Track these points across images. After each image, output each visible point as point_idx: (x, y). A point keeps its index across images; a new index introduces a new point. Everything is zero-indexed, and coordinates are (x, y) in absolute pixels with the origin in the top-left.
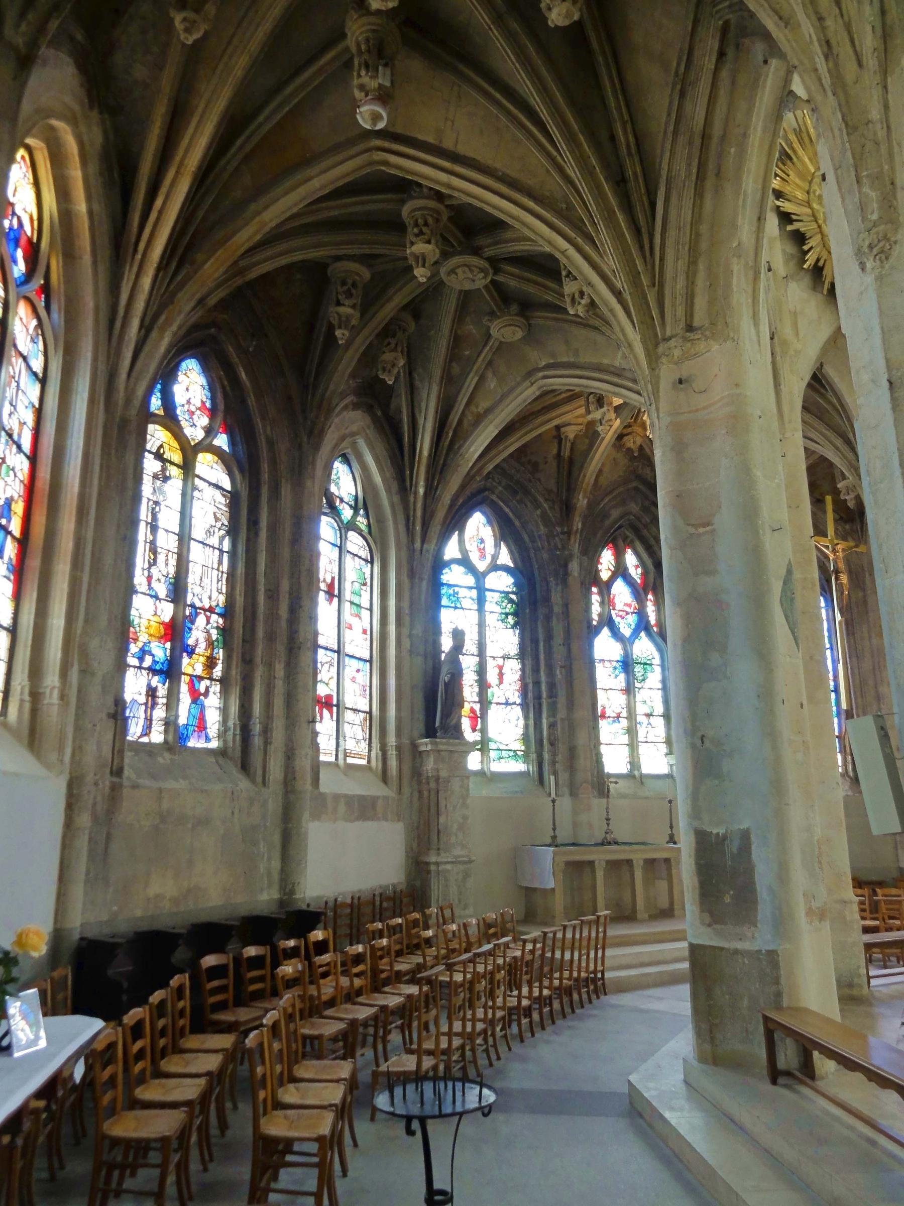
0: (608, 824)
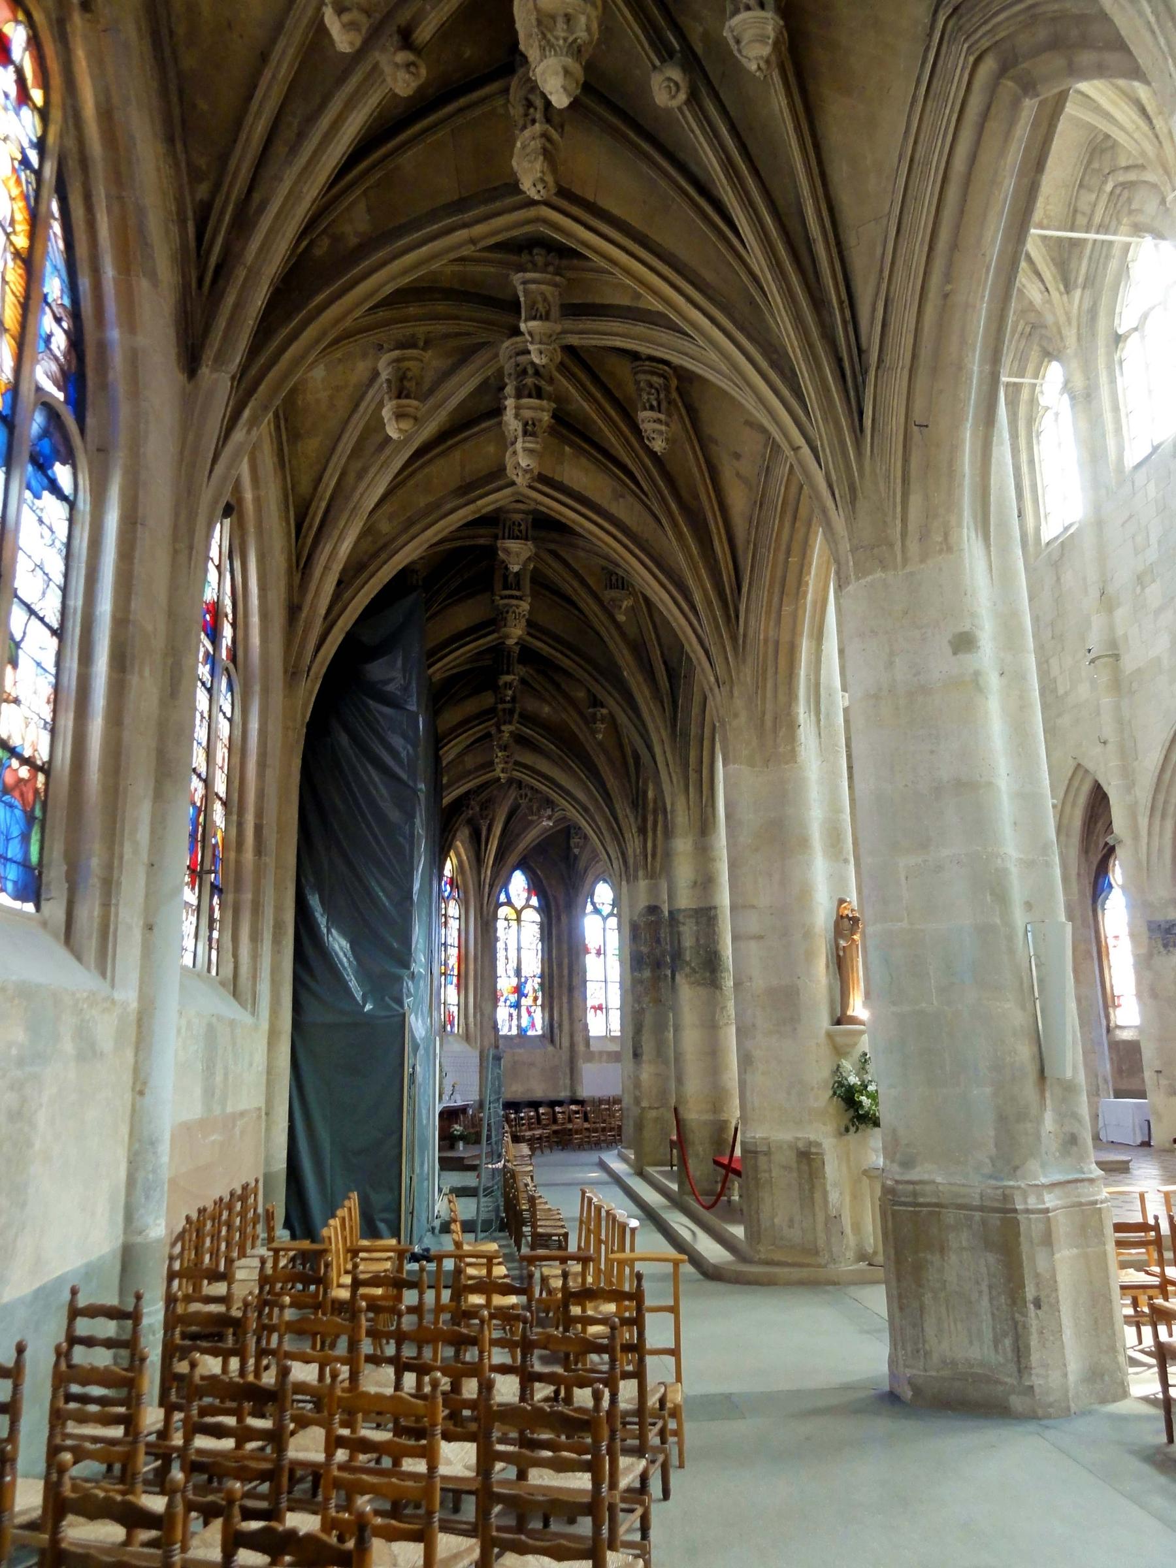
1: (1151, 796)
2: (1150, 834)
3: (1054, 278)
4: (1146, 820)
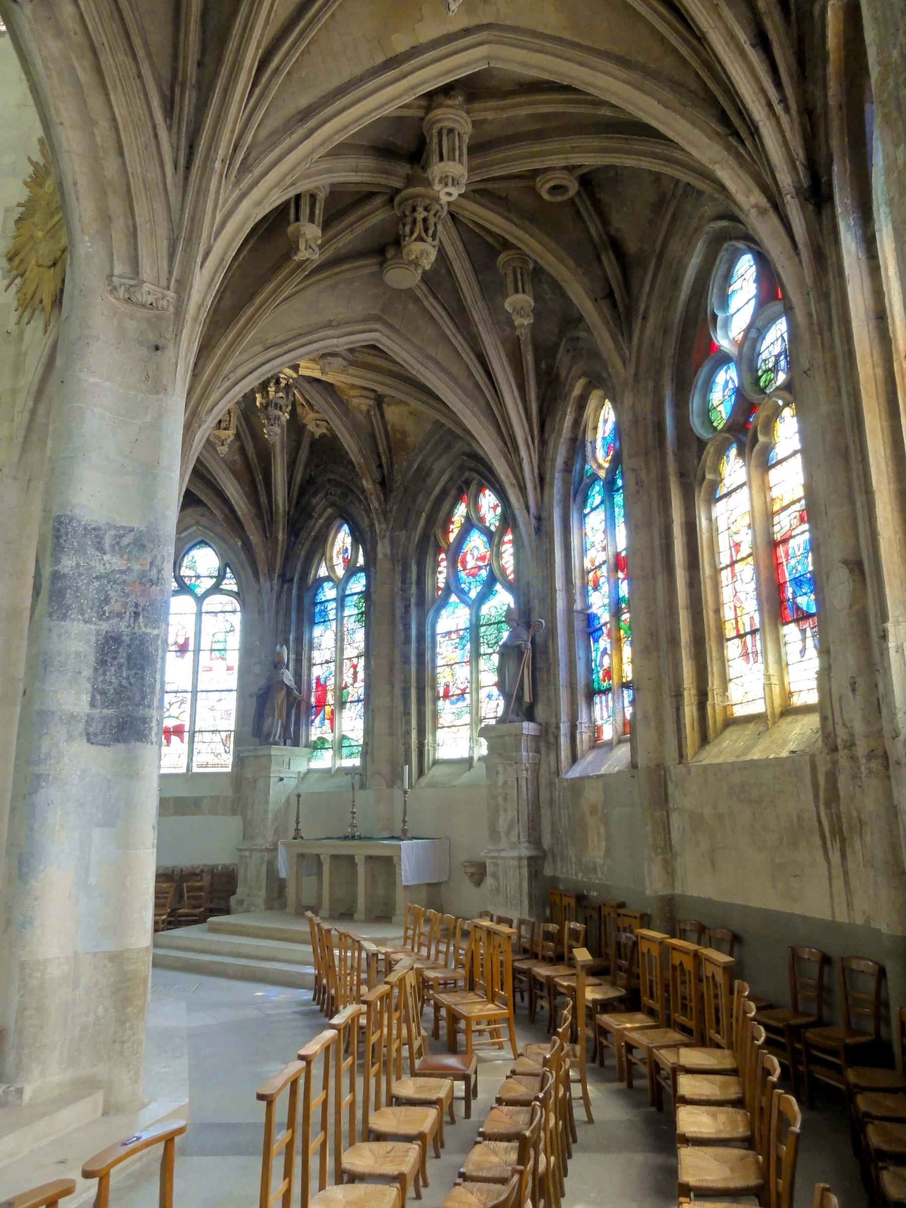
0: (353, 818)
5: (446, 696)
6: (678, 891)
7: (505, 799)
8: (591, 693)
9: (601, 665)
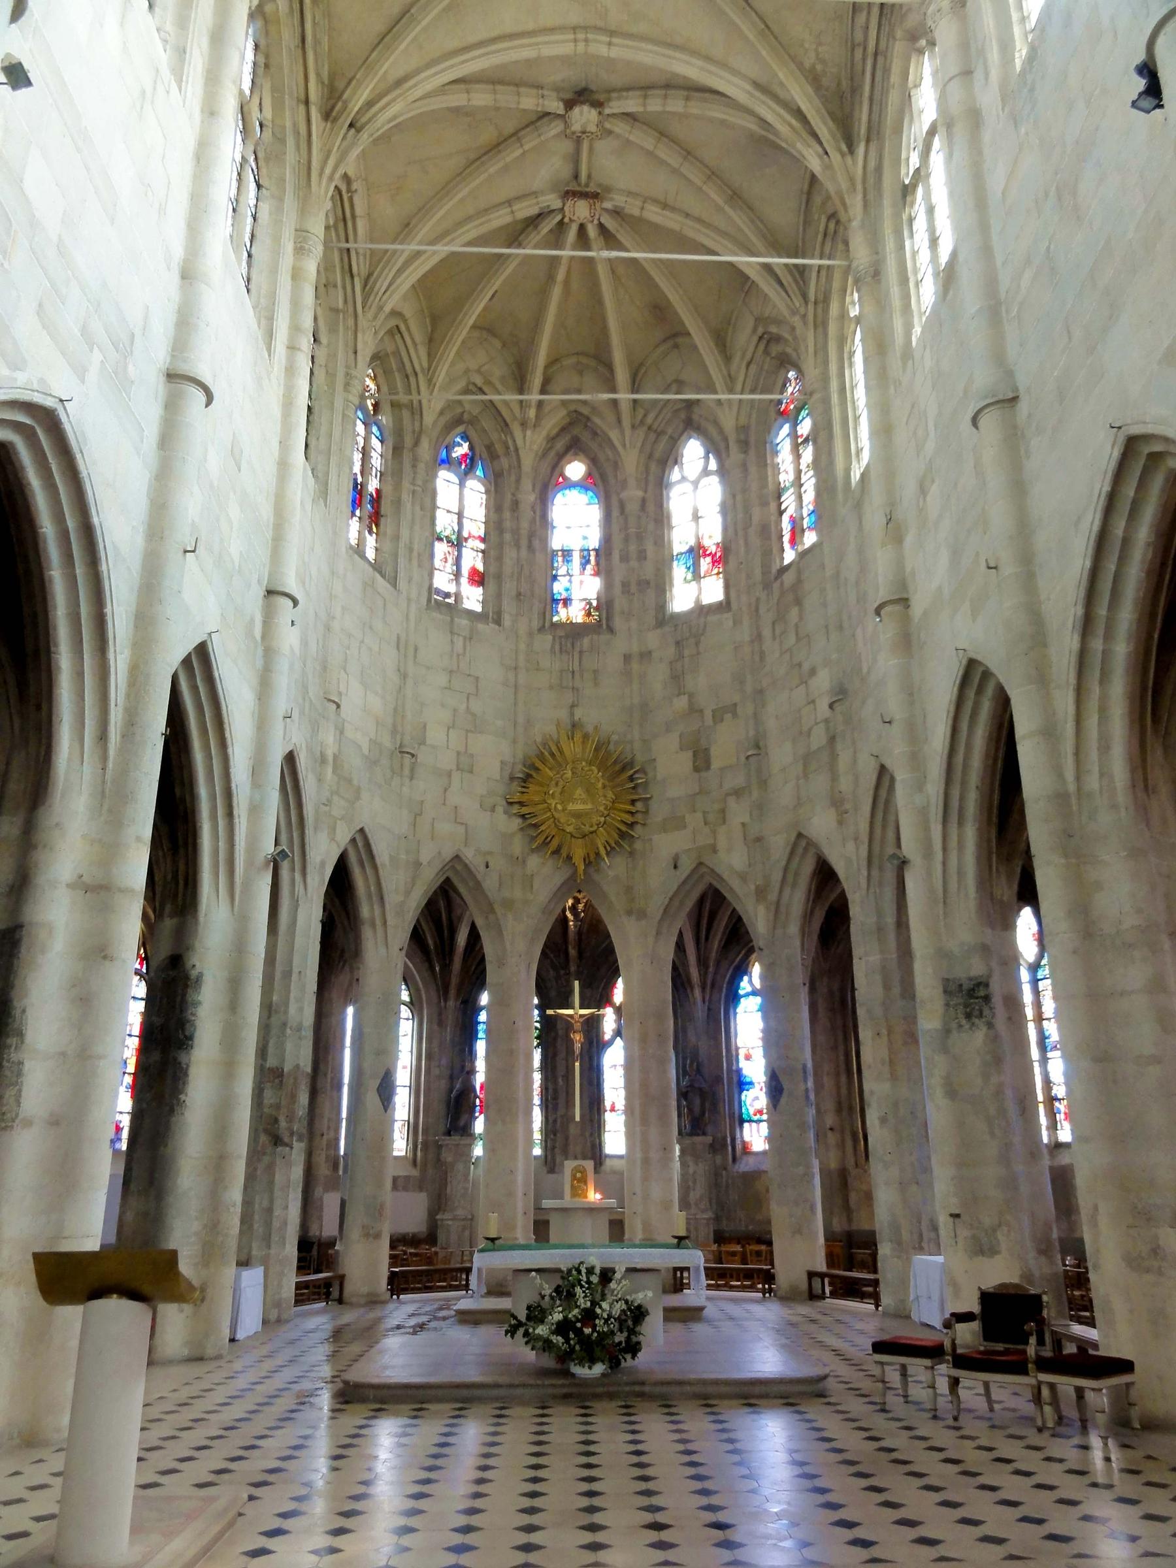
1: (942, 791)
2: (945, 849)
3: (834, 136)
4: (940, 827)
5: (613, 1109)
6: (854, 1227)
7: (695, 1182)
8: (742, 1122)
9: (751, 1105)
